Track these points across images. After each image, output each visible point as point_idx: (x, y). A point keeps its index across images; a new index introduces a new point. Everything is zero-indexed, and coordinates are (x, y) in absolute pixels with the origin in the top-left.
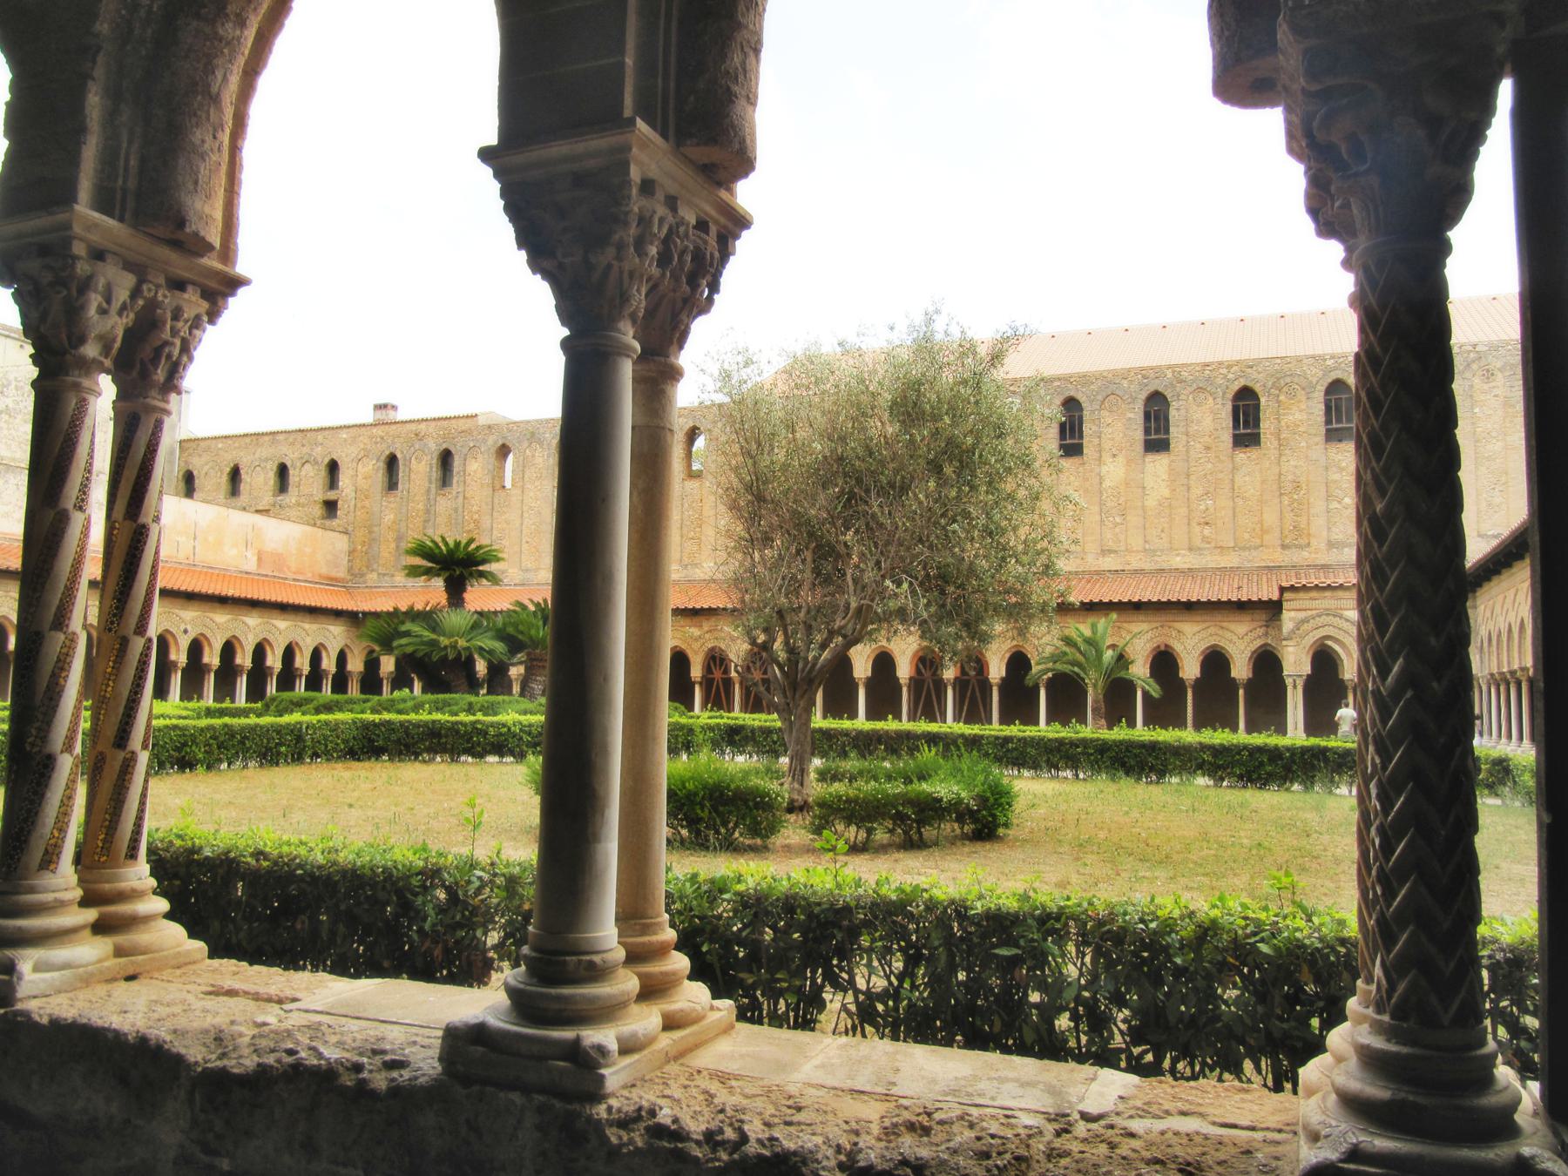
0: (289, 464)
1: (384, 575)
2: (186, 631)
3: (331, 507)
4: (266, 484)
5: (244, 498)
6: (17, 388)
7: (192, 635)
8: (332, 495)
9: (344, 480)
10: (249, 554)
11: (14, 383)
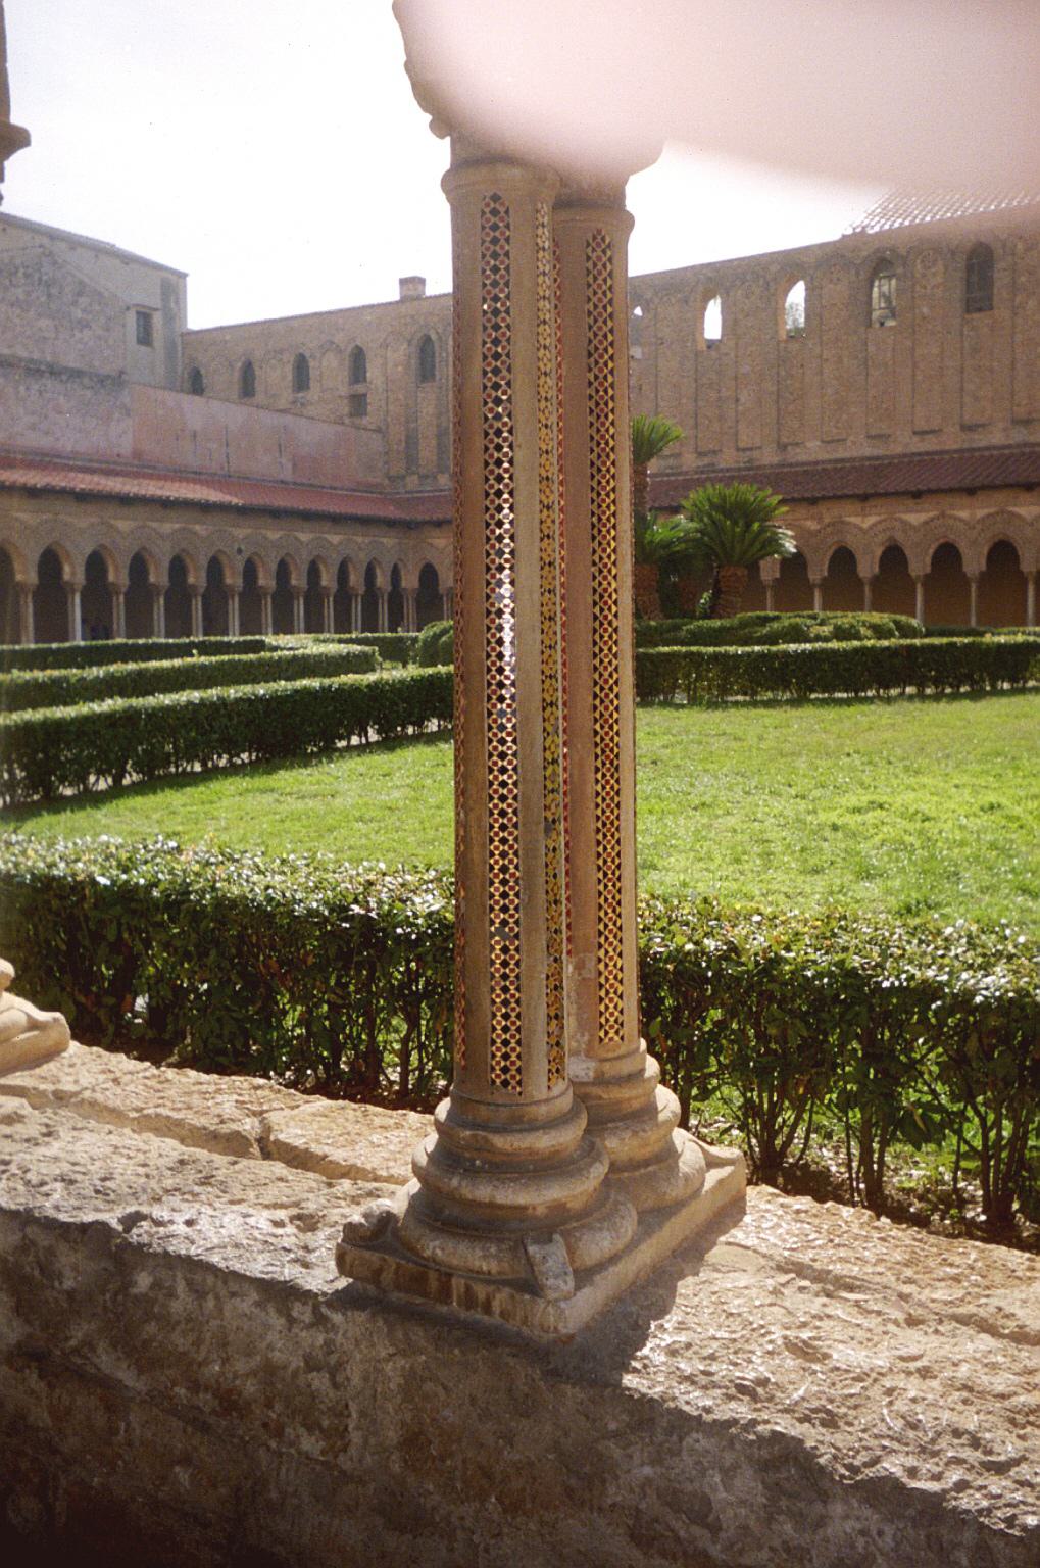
0: (307, 355)
1: (427, 477)
2: (240, 551)
3: (358, 403)
4: (284, 378)
5: (260, 398)
6: (27, 276)
7: (246, 555)
8: (360, 388)
9: (373, 372)
10: (284, 461)
11: (22, 270)
